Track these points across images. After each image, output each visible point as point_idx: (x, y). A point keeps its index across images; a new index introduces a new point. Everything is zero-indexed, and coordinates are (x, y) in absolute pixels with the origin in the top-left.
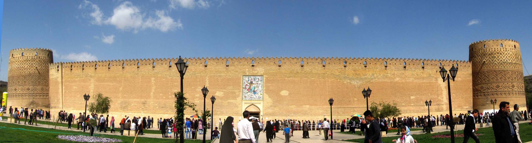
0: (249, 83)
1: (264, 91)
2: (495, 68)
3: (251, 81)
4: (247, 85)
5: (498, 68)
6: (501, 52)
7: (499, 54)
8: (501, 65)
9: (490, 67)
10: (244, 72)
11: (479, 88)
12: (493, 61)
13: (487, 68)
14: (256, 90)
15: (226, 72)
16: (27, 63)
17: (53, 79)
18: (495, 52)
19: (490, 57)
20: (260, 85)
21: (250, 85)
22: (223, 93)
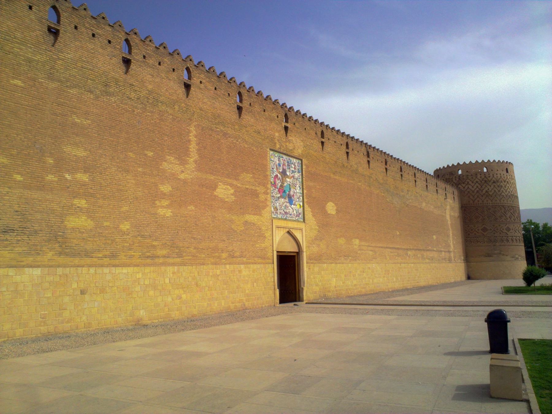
0: (279, 172)
1: (305, 200)
3: (283, 169)
4: (277, 176)
5: (506, 202)
6: (507, 180)
8: (510, 199)
9: (496, 201)
11: (478, 230)
12: (500, 193)
13: (492, 201)
14: (292, 193)
15: (236, 127)
18: (500, 180)
19: (494, 186)
20: (298, 182)
21: (282, 179)
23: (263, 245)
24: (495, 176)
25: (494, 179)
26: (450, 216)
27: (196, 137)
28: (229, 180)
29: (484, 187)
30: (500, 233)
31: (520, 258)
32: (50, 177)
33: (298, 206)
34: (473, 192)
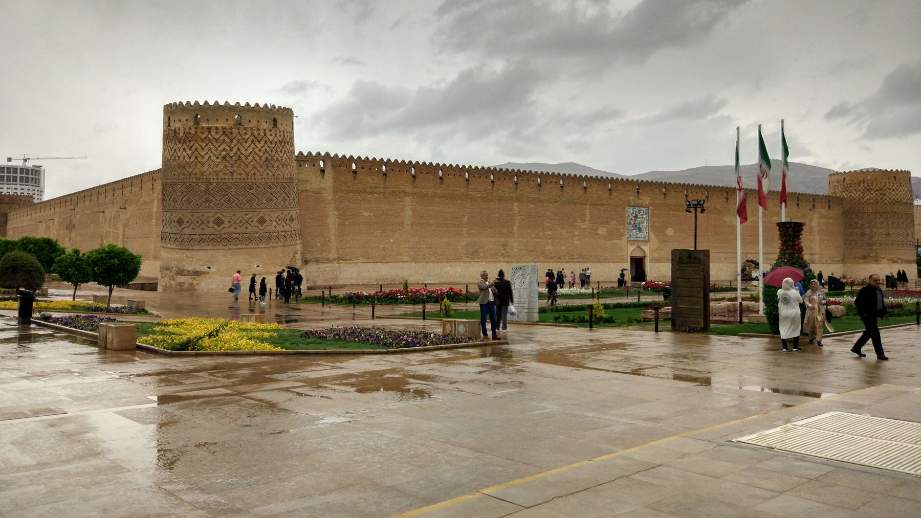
2: (885, 209)
6: (894, 188)
7: (891, 191)
10: (629, 201)
14: (641, 226)
16: (285, 148)
17: (307, 191)
18: (884, 188)
19: (877, 194)
22: (606, 230)
23: (623, 254)
24: (879, 185)
25: (877, 188)
26: (819, 223)
27: (589, 209)
28: (604, 225)
29: (866, 194)
30: (878, 238)
31: (900, 261)
32: (541, 234)
33: (645, 233)
34: (855, 199)
